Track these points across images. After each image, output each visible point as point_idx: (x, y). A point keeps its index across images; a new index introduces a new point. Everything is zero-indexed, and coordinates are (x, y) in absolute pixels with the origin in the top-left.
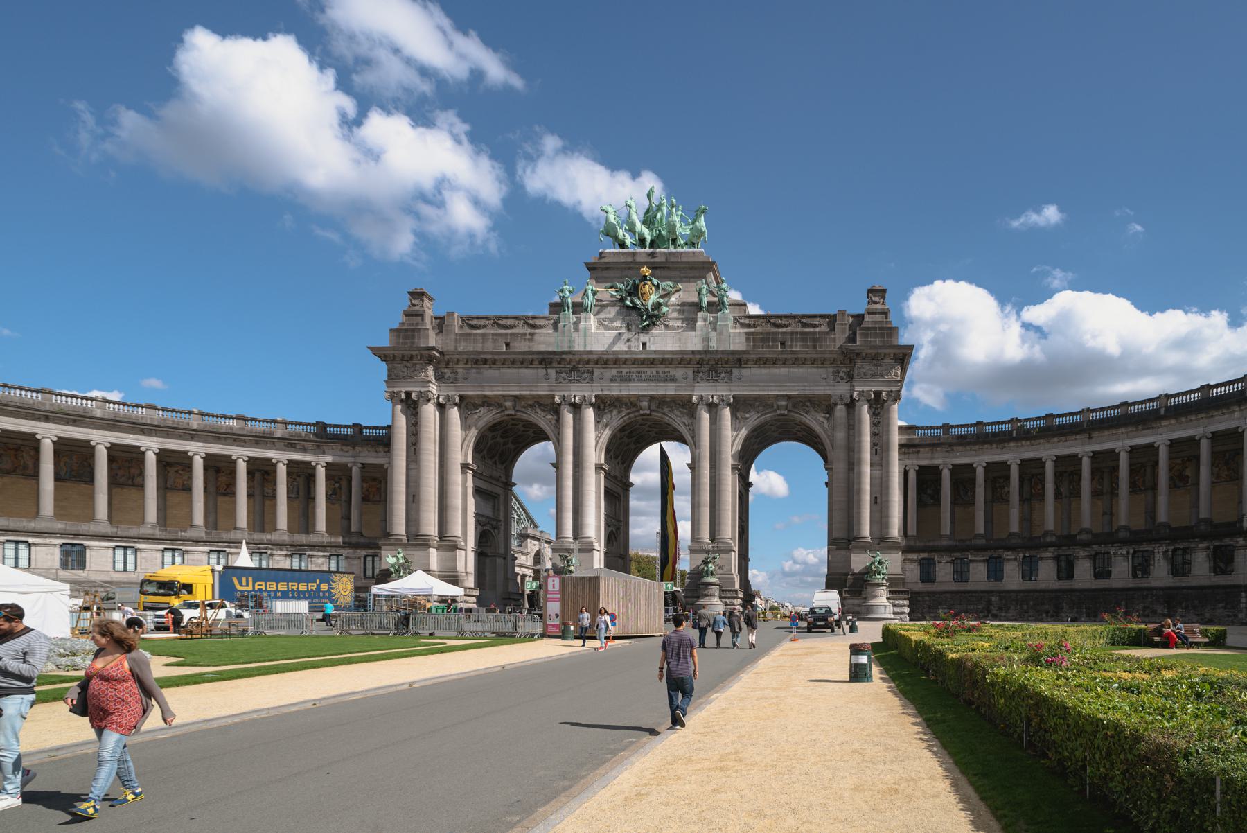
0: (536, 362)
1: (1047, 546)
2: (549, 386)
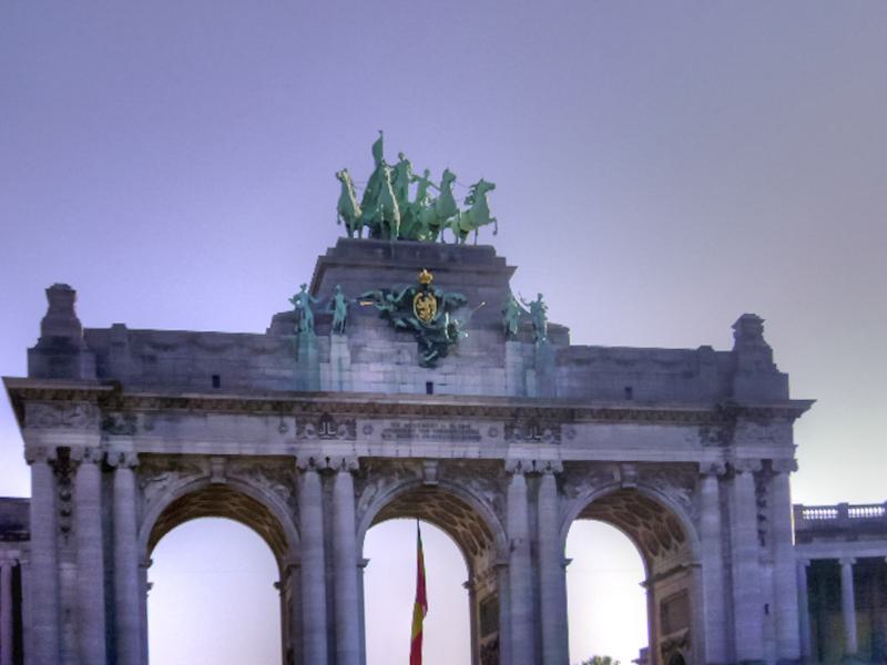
2: (288, 443)
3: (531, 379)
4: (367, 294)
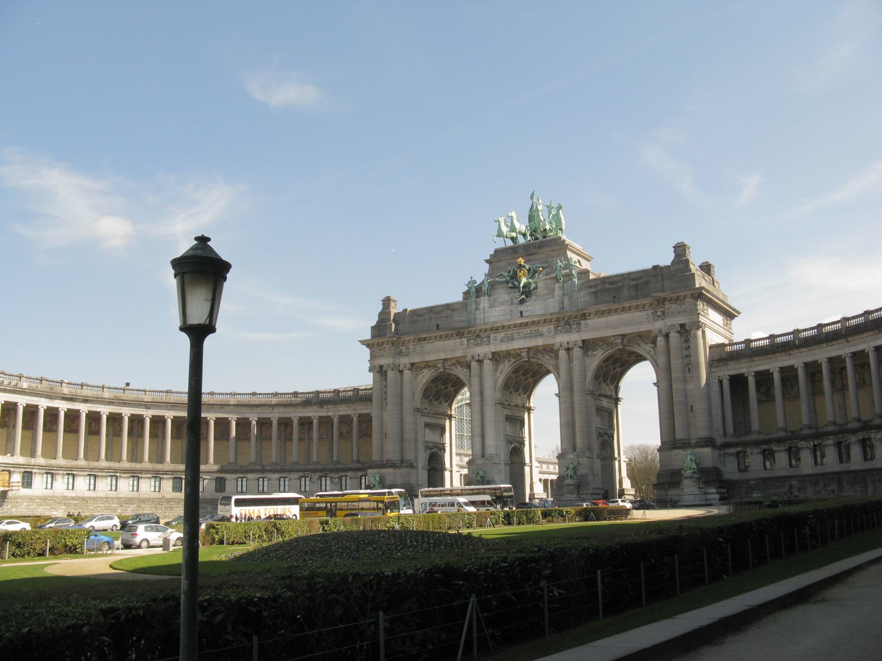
0: (454, 335)
1: (828, 434)
3: (566, 301)
4: (499, 274)
